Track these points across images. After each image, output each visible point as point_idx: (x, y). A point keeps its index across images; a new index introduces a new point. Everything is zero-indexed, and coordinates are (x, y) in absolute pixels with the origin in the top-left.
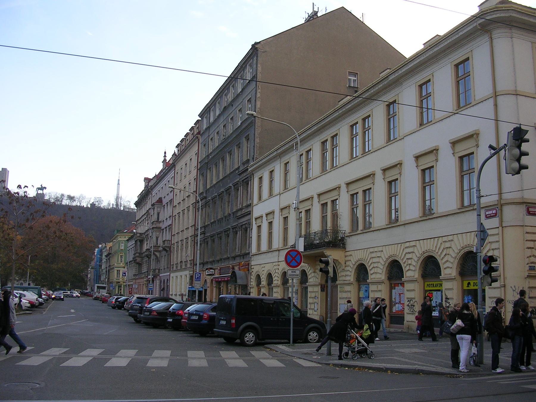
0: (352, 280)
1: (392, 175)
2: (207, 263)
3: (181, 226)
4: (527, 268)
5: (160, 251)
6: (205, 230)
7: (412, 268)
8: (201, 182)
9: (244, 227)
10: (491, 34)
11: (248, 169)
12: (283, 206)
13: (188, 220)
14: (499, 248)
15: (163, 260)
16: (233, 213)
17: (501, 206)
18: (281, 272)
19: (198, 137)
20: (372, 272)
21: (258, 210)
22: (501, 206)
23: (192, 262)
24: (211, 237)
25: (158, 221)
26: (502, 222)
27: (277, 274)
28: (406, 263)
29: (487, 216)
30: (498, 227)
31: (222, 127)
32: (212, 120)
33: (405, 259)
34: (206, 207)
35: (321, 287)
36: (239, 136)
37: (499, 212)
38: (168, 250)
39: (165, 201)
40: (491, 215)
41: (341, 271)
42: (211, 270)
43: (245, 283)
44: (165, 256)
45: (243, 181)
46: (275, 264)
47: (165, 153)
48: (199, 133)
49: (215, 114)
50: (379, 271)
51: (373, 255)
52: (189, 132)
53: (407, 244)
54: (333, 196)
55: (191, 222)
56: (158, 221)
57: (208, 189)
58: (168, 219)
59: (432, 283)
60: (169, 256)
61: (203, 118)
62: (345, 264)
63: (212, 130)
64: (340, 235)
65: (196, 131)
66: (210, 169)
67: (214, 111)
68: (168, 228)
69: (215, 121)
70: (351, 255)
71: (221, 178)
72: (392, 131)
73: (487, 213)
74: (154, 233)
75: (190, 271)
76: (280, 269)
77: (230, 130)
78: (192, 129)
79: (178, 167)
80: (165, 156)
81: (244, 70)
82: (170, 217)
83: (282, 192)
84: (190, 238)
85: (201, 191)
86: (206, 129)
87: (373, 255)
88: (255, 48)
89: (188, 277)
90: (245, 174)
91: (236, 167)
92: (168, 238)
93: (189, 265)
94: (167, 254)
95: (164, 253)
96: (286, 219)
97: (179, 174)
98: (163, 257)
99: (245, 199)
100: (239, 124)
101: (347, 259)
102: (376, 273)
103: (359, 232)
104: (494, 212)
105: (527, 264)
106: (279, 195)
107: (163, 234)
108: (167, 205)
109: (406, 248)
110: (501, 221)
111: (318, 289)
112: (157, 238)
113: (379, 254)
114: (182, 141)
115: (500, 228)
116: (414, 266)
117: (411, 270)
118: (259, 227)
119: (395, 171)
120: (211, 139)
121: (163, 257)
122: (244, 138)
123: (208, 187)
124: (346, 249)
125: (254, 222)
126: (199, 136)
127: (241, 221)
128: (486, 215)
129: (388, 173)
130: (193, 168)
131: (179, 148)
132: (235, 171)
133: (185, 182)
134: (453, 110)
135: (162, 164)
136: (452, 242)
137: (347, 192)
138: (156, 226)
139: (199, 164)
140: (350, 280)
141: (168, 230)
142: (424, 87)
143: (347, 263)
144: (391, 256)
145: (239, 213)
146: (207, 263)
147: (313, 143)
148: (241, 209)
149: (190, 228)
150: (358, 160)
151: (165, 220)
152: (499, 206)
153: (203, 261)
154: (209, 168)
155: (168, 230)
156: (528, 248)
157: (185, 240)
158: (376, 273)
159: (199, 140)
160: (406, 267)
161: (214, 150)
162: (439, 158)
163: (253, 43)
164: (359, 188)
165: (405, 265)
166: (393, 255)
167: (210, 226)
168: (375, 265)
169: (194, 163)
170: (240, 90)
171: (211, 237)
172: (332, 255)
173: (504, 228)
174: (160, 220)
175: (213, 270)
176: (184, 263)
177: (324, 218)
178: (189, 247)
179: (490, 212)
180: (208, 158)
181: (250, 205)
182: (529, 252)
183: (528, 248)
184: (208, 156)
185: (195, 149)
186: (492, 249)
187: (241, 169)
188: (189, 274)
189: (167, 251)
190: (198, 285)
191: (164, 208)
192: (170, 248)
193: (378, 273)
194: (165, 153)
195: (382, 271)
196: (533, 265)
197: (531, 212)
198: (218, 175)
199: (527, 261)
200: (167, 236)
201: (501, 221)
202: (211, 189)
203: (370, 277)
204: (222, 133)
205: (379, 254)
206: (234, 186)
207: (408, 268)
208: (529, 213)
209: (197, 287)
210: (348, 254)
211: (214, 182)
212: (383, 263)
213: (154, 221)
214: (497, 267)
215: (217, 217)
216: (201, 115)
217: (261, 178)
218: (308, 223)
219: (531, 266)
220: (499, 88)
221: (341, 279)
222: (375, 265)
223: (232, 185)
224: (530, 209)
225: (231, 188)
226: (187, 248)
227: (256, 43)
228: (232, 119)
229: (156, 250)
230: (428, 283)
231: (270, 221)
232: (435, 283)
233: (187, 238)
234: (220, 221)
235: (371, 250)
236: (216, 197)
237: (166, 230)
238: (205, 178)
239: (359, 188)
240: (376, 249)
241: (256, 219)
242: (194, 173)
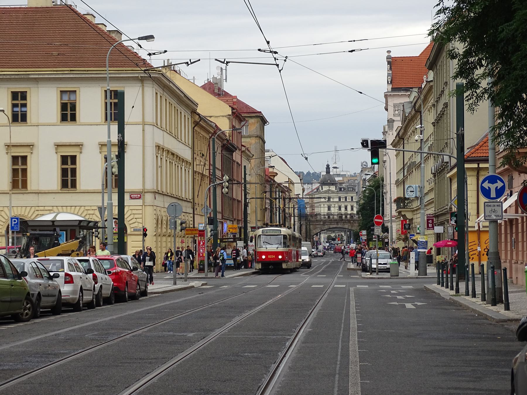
37: (142, 196)
73: (132, 196)
104: (139, 196)
110: (144, 202)
115: (143, 206)
134: (102, 122)
136: (96, 211)
162: (83, 151)
166: (20, 215)
186: (135, 218)
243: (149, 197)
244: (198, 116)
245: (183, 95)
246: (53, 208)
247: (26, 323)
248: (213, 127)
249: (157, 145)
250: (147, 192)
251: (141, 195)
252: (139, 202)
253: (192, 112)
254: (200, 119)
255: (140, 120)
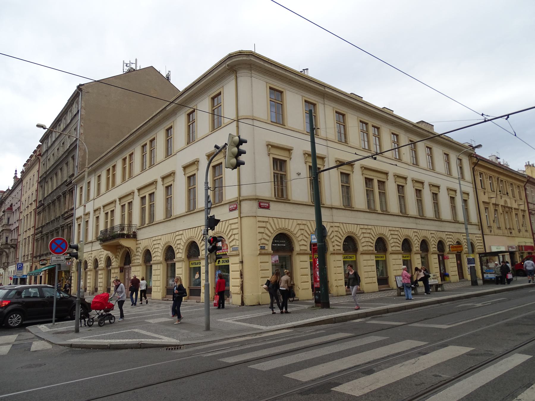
0: (141, 262)
1: (168, 182)
2: (43, 255)
3: (25, 228)
4: (259, 248)
5: (9, 249)
6: (42, 229)
7: (180, 251)
8: (41, 193)
9: (69, 225)
10: (236, 73)
11: (72, 181)
12: (96, 208)
13: (31, 222)
14: (238, 234)
15: (12, 255)
16: (62, 215)
17: (240, 202)
18: (93, 259)
19: (39, 158)
20: (154, 255)
21: (79, 212)
22: (240, 202)
23: (32, 255)
24: (46, 235)
25: (8, 224)
26: (240, 213)
27: (90, 261)
28: (177, 248)
29: (231, 209)
30: (238, 218)
31: (56, 149)
32: (49, 144)
33: (176, 244)
34: (43, 211)
35: (120, 269)
36: (67, 157)
37: (238, 206)
38: (15, 247)
39: (14, 208)
40: (233, 208)
41: (134, 256)
42: (44, 261)
43: (68, 269)
44: (13, 251)
45: (69, 190)
46: (89, 253)
47: (16, 171)
48: (40, 155)
49: (51, 140)
50: (159, 254)
51: (155, 242)
52: (33, 154)
53: (177, 233)
54: (129, 199)
55: (32, 225)
56: (8, 224)
57: (46, 197)
58: (16, 222)
59: (195, 262)
60: (16, 251)
61: (43, 143)
62: (136, 250)
63: (49, 152)
64: (134, 229)
65: (38, 153)
66: (47, 182)
67: (52, 137)
68: (16, 229)
69: (52, 145)
70: (140, 243)
71: (55, 188)
72: (169, 149)
73: (230, 207)
74: (4, 234)
75: (30, 263)
76: (93, 256)
77: (61, 152)
78: (35, 152)
79: (24, 182)
80: (16, 174)
81: (72, 106)
82: (17, 221)
83: (95, 197)
84: (31, 236)
85: (40, 199)
86: (45, 152)
87: (155, 242)
88: (80, 88)
89: (29, 267)
90: (71, 185)
91: (65, 179)
92: (16, 237)
93: (29, 258)
94: (14, 250)
95: (12, 249)
96: (98, 218)
97: (25, 187)
98: (12, 253)
99: (71, 204)
100: (68, 147)
101: (138, 246)
102: (157, 256)
103: (145, 225)
104: (235, 206)
105: (259, 245)
106: (93, 200)
107: (12, 234)
108: (16, 212)
109: (176, 236)
110: (240, 213)
111: (117, 271)
112: (7, 238)
113: (158, 242)
114: (28, 161)
115: (239, 218)
116: (182, 249)
117: (180, 253)
118: (79, 225)
119: (171, 179)
120: (49, 160)
121: (12, 253)
122: (71, 158)
123: (45, 196)
124: (137, 238)
125: (76, 221)
126: (40, 157)
127: (67, 221)
128: (230, 209)
129: (166, 181)
130: (35, 182)
131: (26, 167)
132: (64, 183)
133: (29, 193)
135: (13, 179)
137: (139, 195)
138: (6, 228)
139: (39, 179)
140: (139, 263)
141: (16, 232)
142: (191, 116)
143: (138, 250)
144: (167, 243)
145: (66, 215)
146: (43, 255)
147: (116, 160)
148: (67, 212)
149: (32, 228)
150: (146, 172)
151: (14, 224)
152: (238, 202)
153: (40, 253)
154: (46, 181)
155: (16, 232)
156: (259, 233)
157: (27, 238)
158: (157, 256)
159: (40, 160)
160: (176, 250)
161: (50, 168)
162: (200, 168)
163: (78, 85)
164: (146, 193)
165: (176, 249)
167: (46, 226)
168: (156, 250)
169: (36, 178)
170: (69, 121)
171: (46, 235)
172: (125, 243)
173: (242, 218)
174: (10, 223)
175: (46, 261)
176: (26, 256)
177: (123, 216)
178: (30, 244)
179: (232, 207)
180: (46, 174)
181: (73, 208)
182: (260, 236)
183: (259, 233)
184: (46, 172)
185: (37, 167)
187: (68, 181)
188: (30, 265)
189: (14, 248)
190: (20, 274)
191: (14, 214)
192: (16, 245)
193: (158, 256)
194: (16, 171)
195: (160, 254)
196: (263, 245)
197: (262, 206)
198: (52, 186)
199: (259, 242)
200: (15, 236)
201: (240, 213)
202: (48, 198)
203: (153, 259)
204: (56, 154)
205: (158, 242)
206: (63, 194)
207: (177, 251)
208: (260, 207)
209: (19, 275)
210: (138, 242)
211: (50, 192)
212: (161, 248)
213: (4, 225)
214: (237, 248)
215: (51, 219)
216: (42, 141)
217: (81, 188)
218: (112, 221)
219: (261, 247)
220: (242, 114)
221: (136, 261)
222: (156, 250)
223: (61, 194)
224: (261, 204)
225: (61, 196)
226: (29, 244)
227: (80, 85)
228: (63, 143)
229: (6, 247)
230: (192, 262)
231: (86, 220)
232: (196, 262)
233: (29, 237)
234: (52, 222)
235: (154, 239)
236: (50, 203)
237: (14, 231)
238: (44, 189)
239: (146, 193)
240: (157, 238)
241: (77, 219)
242: (36, 185)
243: (247, 207)
244: (475, 159)
245: (412, 126)
246: (183, 232)
247: (344, 323)
248: (525, 177)
249: (304, 153)
250: (243, 200)
251: (237, 206)
252: (236, 213)
253: (469, 155)
254: (477, 160)
255: (234, 117)
